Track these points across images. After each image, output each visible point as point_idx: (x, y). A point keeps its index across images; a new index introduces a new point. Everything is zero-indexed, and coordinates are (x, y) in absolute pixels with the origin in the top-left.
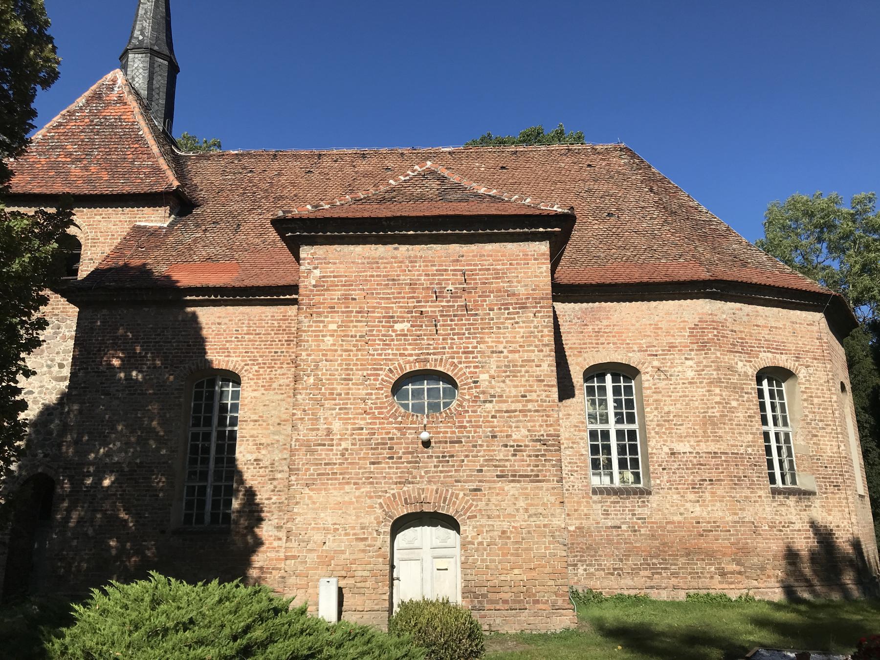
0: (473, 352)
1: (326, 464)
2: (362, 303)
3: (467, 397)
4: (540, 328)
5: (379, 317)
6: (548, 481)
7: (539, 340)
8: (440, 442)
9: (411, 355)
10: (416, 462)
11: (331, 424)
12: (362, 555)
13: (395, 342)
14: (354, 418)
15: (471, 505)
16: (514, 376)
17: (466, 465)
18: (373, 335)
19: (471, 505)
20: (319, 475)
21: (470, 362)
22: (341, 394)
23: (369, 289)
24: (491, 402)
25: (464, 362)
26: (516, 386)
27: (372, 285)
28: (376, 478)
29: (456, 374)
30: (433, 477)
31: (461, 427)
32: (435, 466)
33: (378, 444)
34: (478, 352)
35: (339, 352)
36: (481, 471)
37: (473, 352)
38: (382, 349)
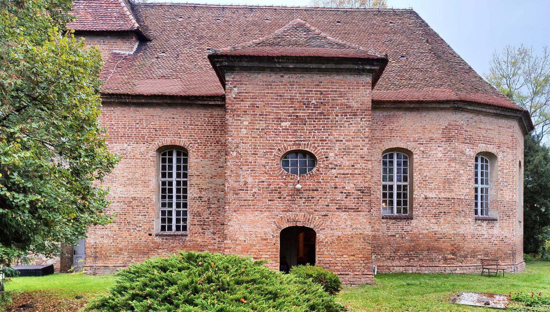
0: (325, 140)
1: (244, 200)
2: (263, 109)
3: (322, 166)
4: (364, 128)
5: (273, 118)
6: (364, 211)
7: (363, 135)
8: (306, 190)
9: (291, 141)
10: (293, 200)
11: (247, 178)
12: (265, 248)
13: (282, 133)
14: (259, 176)
15: (323, 223)
16: (348, 155)
17: (320, 203)
18: (269, 129)
19: (323, 223)
20: (240, 206)
21: (324, 146)
22: (251, 163)
23: (266, 101)
24: (335, 169)
25: (321, 146)
26: (348, 160)
27: (268, 99)
28: (272, 208)
29: (316, 153)
30: (303, 208)
31: (318, 182)
32: (304, 203)
33: (273, 190)
34: (329, 140)
35: (250, 138)
36: (328, 206)
37: (325, 140)
38: (274, 137)
